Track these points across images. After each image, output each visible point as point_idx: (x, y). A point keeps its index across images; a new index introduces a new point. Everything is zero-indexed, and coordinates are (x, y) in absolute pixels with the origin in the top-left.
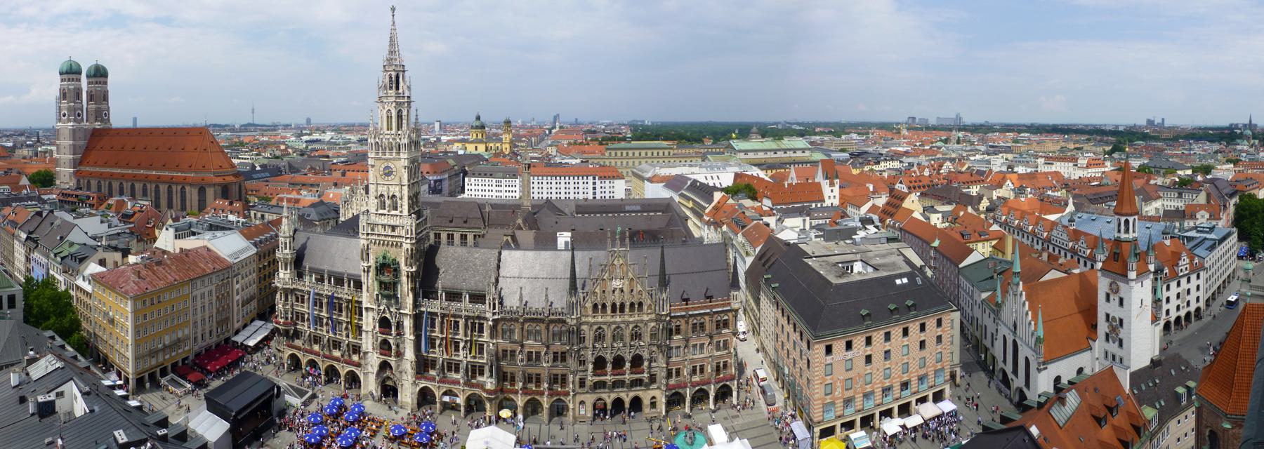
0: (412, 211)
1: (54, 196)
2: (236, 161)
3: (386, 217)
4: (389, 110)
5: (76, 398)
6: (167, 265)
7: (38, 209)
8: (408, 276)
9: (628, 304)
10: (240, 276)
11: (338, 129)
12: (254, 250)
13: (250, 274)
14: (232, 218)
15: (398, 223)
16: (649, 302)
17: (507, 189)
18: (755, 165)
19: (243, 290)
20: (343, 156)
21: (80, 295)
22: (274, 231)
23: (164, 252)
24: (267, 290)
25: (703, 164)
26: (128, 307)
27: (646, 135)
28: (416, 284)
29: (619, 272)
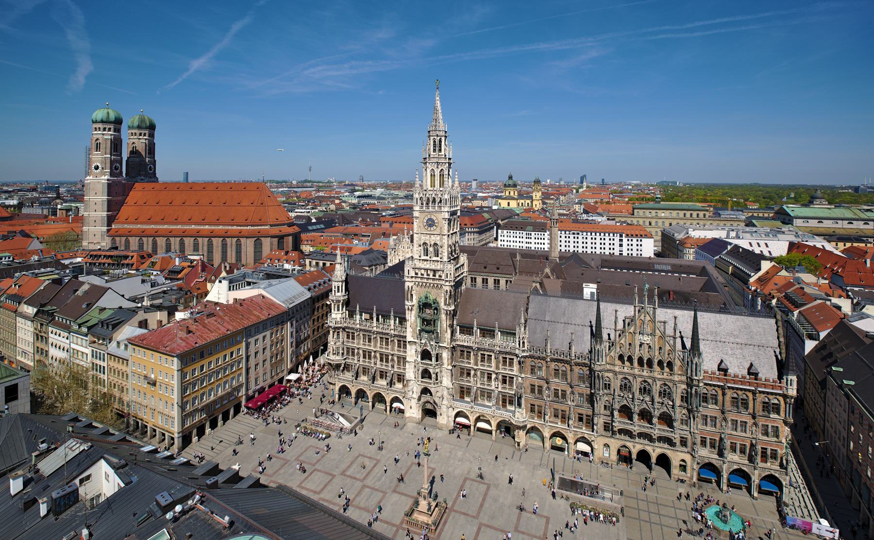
3: (429, 262)
6: (220, 317)
13: (305, 317)
15: (439, 268)
23: (216, 304)
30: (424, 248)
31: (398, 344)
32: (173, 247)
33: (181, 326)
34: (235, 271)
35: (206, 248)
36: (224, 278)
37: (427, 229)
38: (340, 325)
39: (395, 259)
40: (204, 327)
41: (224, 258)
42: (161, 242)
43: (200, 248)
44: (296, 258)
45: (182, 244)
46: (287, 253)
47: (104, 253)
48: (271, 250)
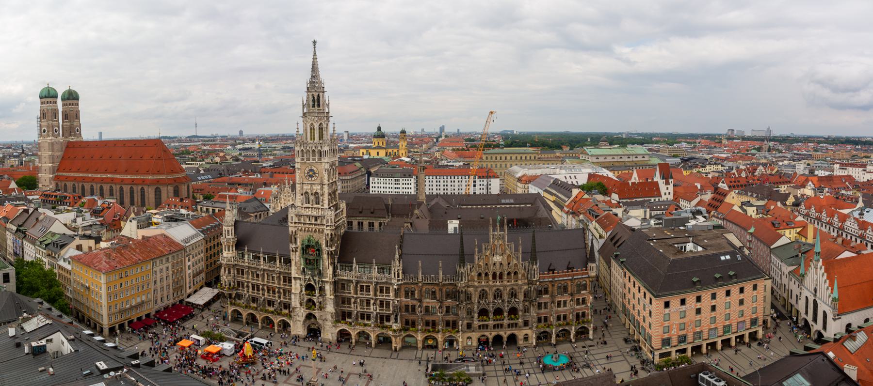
0: (331, 205)
1: (38, 197)
2: (184, 166)
3: (310, 209)
5: (63, 343)
7: (25, 208)
8: (328, 254)
9: (506, 273)
10: (191, 256)
11: (266, 140)
12: (201, 237)
13: (199, 254)
14: (183, 211)
15: (320, 214)
16: (523, 271)
17: (404, 186)
18: (604, 167)
19: (193, 266)
20: (270, 160)
21: (61, 272)
22: (218, 221)
23: (130, 239)
24: (213, 266)
25: (563, 166)
26: (103, 279)
27: (516, 142)
28: (334, 260)
29: (499, 251)
30: (306, 197)
34: (141, 213)
37: (310, 179)
38: (230, 263)
40: (121, 255)
41: (132, 203)
47: (52, 194)
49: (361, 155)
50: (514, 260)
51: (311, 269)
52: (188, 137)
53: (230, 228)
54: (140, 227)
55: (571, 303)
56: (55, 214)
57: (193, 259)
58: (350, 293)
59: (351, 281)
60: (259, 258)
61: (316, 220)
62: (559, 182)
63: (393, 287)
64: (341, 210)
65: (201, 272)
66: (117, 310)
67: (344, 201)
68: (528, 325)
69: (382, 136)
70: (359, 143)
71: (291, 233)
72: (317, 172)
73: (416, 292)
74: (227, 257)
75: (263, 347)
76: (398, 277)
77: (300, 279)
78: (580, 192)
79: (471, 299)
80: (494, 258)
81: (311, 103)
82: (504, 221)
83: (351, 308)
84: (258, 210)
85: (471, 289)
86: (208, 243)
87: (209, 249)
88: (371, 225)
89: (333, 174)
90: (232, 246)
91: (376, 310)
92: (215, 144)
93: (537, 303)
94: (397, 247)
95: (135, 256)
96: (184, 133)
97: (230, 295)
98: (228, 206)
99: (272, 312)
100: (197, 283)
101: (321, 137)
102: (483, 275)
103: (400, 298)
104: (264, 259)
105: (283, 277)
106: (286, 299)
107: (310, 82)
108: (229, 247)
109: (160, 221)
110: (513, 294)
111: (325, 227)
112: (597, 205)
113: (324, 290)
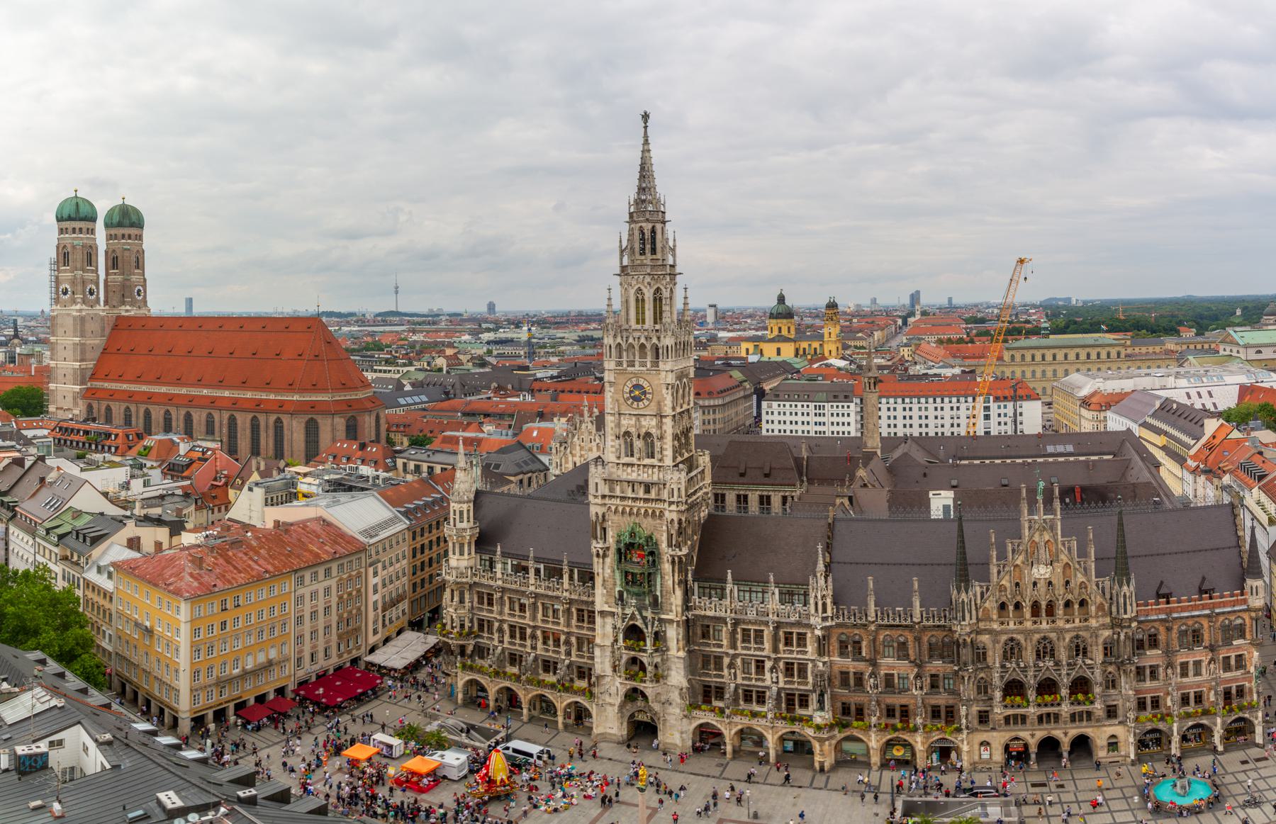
0: (679, 459)
2: (370, 376)
3: (635, 468)
4: (639, 289)
8: (673, 562)
9: (1061, 603)
10: (380, 565)
12: (404, 524)
13: (398, 561)
15: (655, 478)
16: (1099, 599)
17: (835, 419)
19: (384, 585)
21: (90, 594)
23: (246, 527)
24: (427, 585)
25: (1182, 370)
27: (1075, 323)
28: (686, 576)
31: (578, 615)
32: (174, 424)
33: (190, 555)
34: (275, 473)
35: (225, 430)
36: (257, 484)
38: (464, 580)
39: (567, 462)
40: (228, 562)
41: (255, 451)
42: (157, 413)
43: (217, 429)
44: (379, 457)
45: (188, 419)
46: (363, 447)
48: (334, 441)
49: (743, 354)
50: (1079, 575)
51: (637, 595)
52: (379, 315)
53: (465, 507)
54: (269, 502)
55: (1212, 666)
56: (82, 470)
57: (385, 572)
58: (721, 646)
59: (722, 620)
60: (526, 569)
61: (647, 491)
62: (1175, 406)
63: (813, 633)
64: (700, 469)
65: (400, 599)
66: (212, 680)
67: (707, 452)
68: (1115, 717)
69: (789, 314)
70: (739, 330)
71: (594, 518)
72: (648, 389)
73: (864, 644)
74: (457, 568)
75: (531, 760)
76: (825, 610)
77: (613, 614)
78: (1222, 425)
79: (985, 659)
80: (1035, 570)
81: (637, 246)
82: (1052, 491)
83: (722, 677)
84: (526, 468)
85: (985, 638)
86: (418, 538)
87: (419, 551)
88: (765, 501)
89: (683, 396)
90: (469, 543)
91: (777, 683)
92: (437, 331)
93: (1133, 668)
94: (820, 547)
95: (256, 562)
96: (372, 306)
97: (462, 649)
98: (461, 461)
99: (553, 686)
100: (391, 621)
101: (658, 317)
102: (1011, 608)
103: (829, 656)
104: (537, 571)
105: (578, 610)
106: (582, 657)
107: (635, 201)
108: (462, 546)
109: (314, 489)
110: (1080, 649)
111: (666, 505)
112: (1261, 453)
113: (665, 639)
